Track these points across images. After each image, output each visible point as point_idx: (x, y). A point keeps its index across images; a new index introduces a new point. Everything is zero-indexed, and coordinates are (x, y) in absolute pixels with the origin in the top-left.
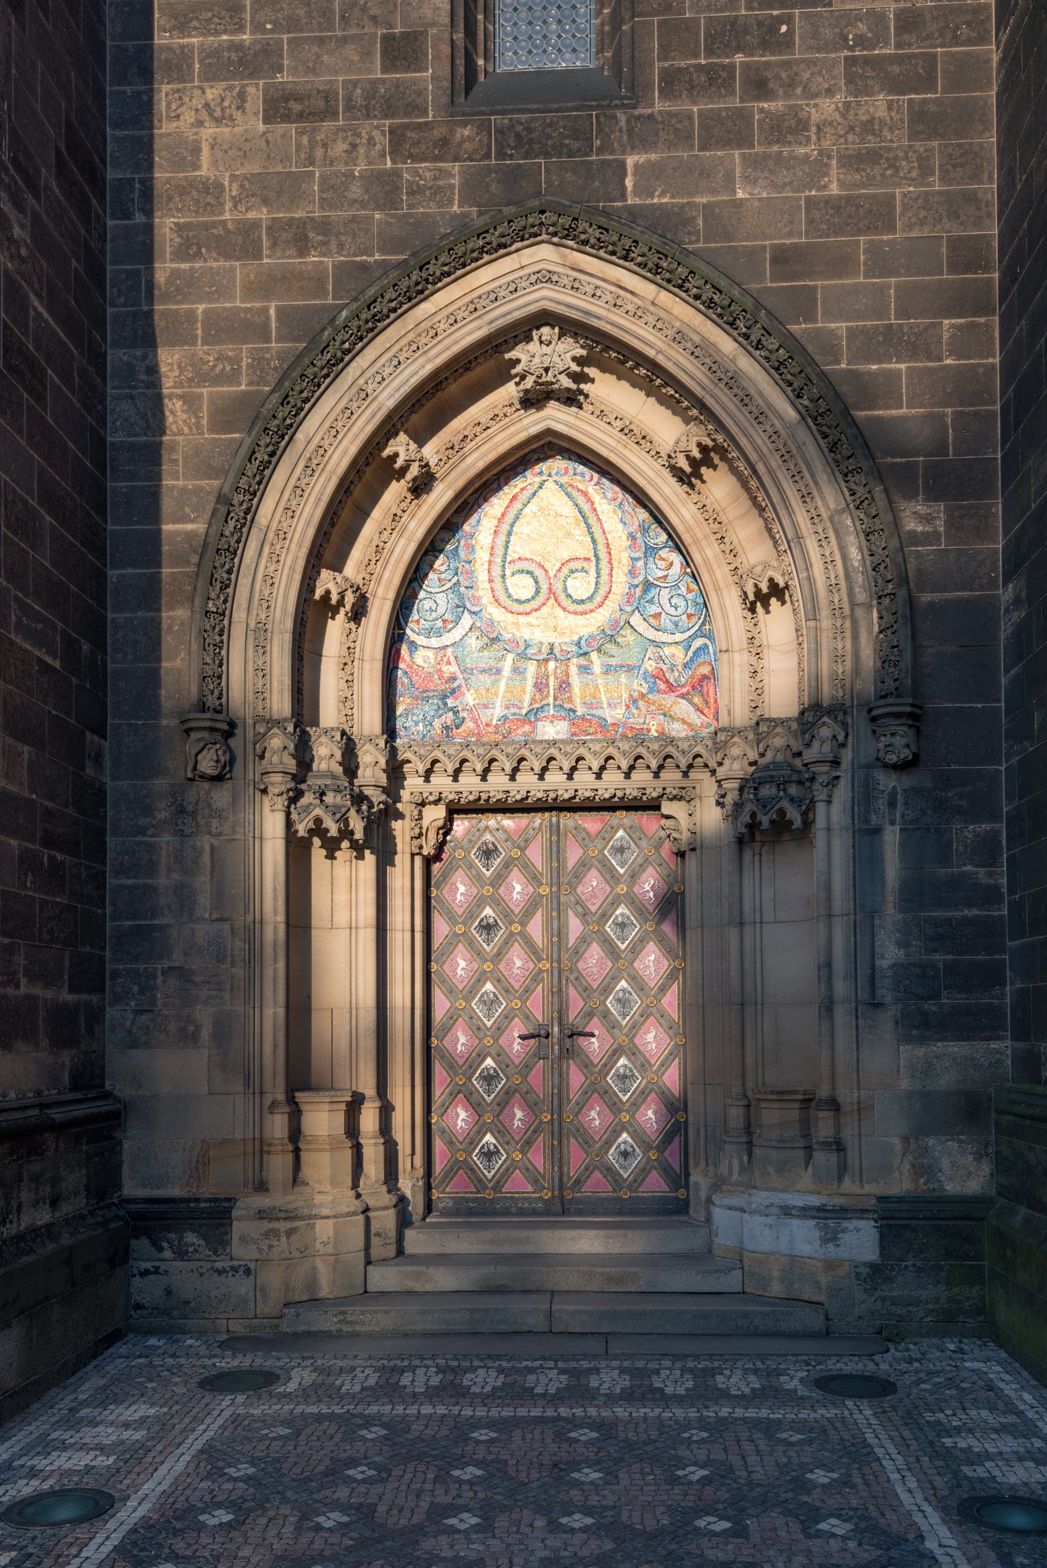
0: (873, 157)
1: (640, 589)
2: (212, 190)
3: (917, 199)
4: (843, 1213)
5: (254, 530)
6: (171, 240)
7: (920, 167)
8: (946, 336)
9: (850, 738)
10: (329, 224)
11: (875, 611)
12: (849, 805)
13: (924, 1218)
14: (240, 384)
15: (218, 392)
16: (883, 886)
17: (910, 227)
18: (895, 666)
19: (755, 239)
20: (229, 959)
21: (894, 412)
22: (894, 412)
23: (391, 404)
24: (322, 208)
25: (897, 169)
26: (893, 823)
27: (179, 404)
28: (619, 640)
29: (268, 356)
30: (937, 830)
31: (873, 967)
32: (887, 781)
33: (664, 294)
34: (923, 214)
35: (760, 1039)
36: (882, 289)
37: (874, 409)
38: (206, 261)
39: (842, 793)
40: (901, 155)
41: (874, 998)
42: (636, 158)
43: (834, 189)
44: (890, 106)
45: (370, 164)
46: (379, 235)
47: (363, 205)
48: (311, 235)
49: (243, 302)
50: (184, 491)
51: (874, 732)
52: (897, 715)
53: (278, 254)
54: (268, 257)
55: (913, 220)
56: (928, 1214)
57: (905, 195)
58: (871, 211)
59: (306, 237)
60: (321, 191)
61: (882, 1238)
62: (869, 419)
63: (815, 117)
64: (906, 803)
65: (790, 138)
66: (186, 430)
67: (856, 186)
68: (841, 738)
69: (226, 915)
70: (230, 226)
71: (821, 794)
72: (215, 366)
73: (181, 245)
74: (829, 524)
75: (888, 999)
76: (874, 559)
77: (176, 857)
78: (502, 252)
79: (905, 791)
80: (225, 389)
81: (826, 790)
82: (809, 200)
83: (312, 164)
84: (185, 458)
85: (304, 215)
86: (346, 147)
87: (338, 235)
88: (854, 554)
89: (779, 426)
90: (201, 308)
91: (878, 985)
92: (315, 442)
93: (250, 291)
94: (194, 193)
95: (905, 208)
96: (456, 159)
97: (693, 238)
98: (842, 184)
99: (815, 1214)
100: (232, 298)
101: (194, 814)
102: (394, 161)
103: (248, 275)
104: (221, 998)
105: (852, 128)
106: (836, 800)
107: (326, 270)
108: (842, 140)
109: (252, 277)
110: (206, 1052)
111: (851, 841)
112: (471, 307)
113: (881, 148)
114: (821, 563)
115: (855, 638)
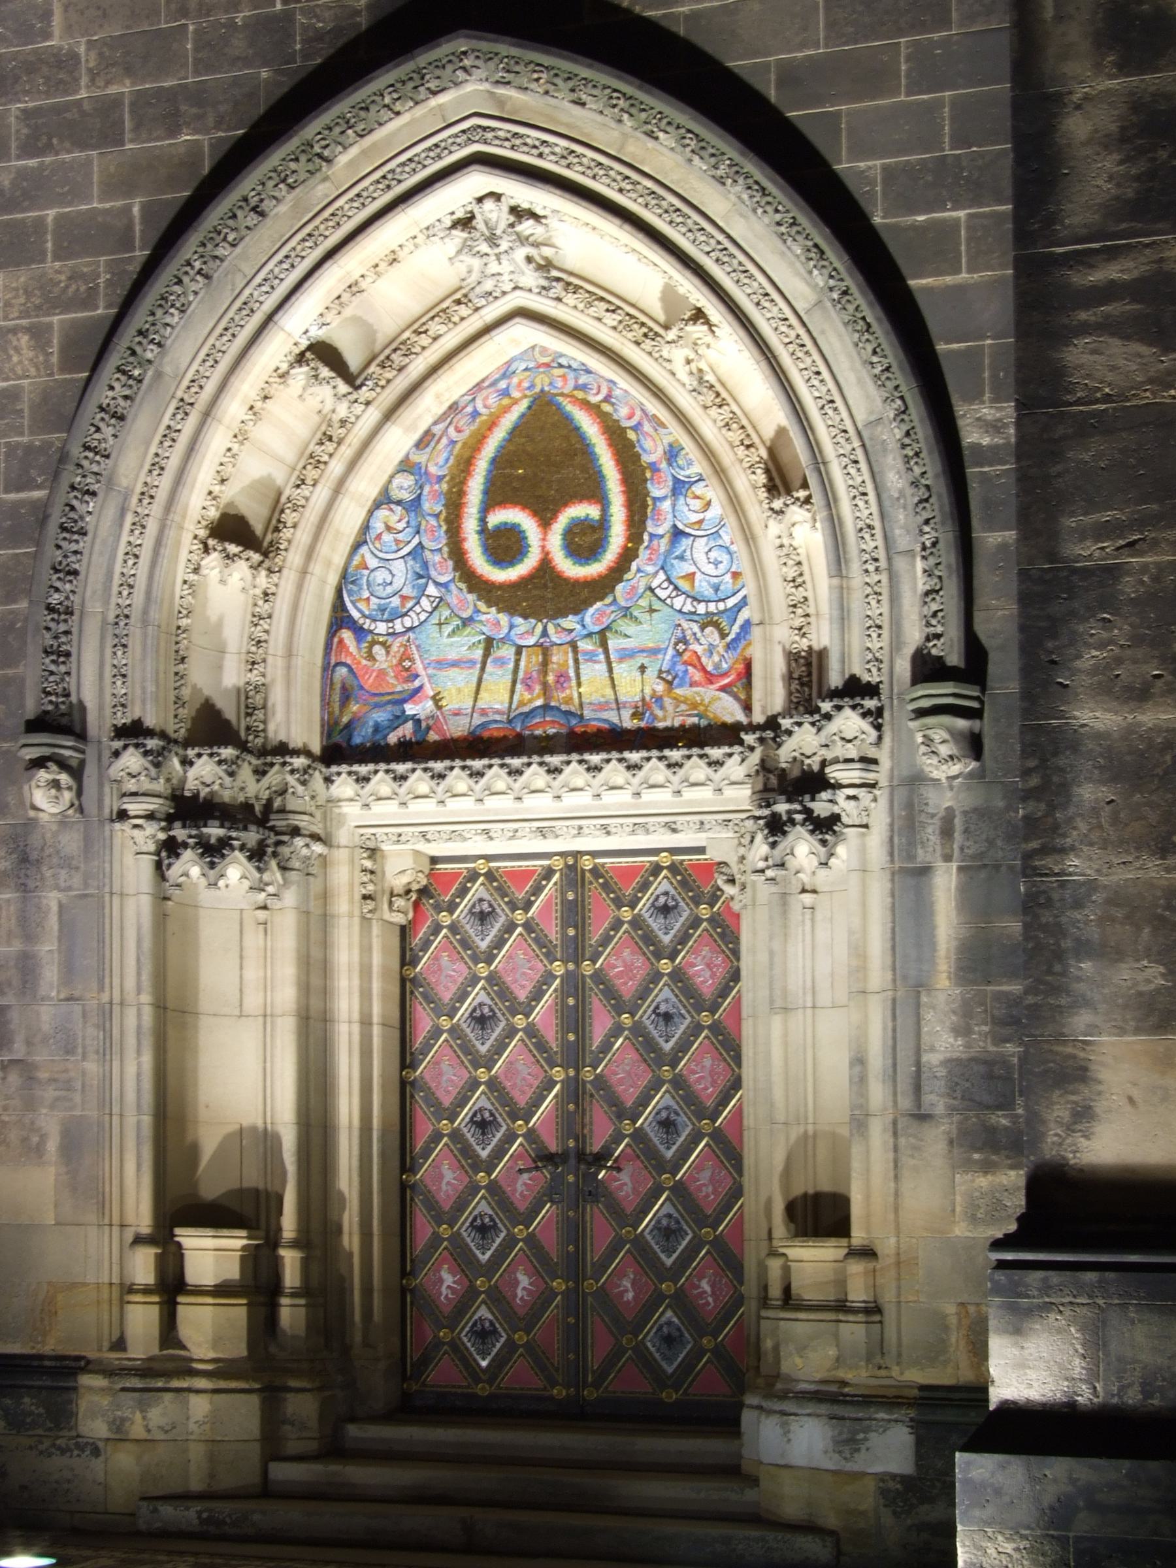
2: (66, 62)
6: (18, 131)
14: (97, 308)
21: (949, 280)
22: (949, 280)
26: (948, 858)
31: (918, 1064)
41: (919, 1107)
49: (101, 201)
54: (132, 141)
64: (966, 831)
70: (86, 106)
72: (67, 287)
73: (27, 136)
79: (965, 813)
88: (895, 480)
90: (51, 214)
91: (925, 1088)
94: (45, 70)
100: (88, 198)
111: (889, 885)
115: (895, 599)
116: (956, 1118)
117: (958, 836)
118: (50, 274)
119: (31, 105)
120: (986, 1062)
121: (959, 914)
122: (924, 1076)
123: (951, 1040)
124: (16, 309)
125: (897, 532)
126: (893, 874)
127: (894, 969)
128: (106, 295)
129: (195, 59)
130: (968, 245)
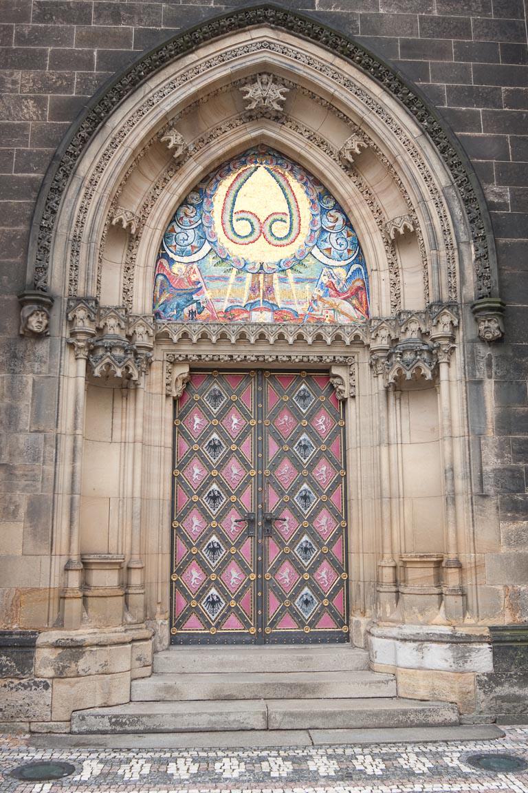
1: (318, 232)
3: (482, 23)
4: (468, 640)
5: (75, 179)
6: (34, 11)
8: (503, 96)
9: (461, 323)
10: (133, 8)
11: (472, 246)
12: (463, 365)
13: (522, 641)
14: (72, 93)
16: (486, 418)
17: (479, 36)
18: (487, 279)
19: (392, 35)
20: (42, 459)
21: (477, 134)
22: (477, 134)
23: (168, 108)
25: (470, 7)
26: (490, 377)
28: (306, 263)
29: (91, 78)
30: (517, 383)
31: (481, 471)
32: (484, 351)
34: (486, 30)
35: (402, 521)
36: (466, 68)
37: (465, 131)
38: (55, 23)
39: (458, 356)
41: (483, 492)
43: (435, 13)
48: (122, 13)
49: (76, 47)
50: (30, 153)
51: (476, 320)
52: (491, 309)
53: (101, 22)
54: (94, 23)
55: (481, 33)
56: (523, 638)
57: (475, 20)
58: (456, 26)
61: (494, 655)
62: (461, 136)
66: (35, 117)
67: (446, 13)
68: (455, 323)
69: (41, 428)
71: (443, 359)
72: (56, 82)
74: (441, 194)
75: (492, 492)
76: (473, 215)
77: (8, 387)
78: (240, 29)
79: (496, 357)
80: (62, 95)
81: (447, 356)
82: (421, 18)
84: (33, 135)
87: (139, 14)
89: (409, 136)
90: (50, 49)
91: (485, 483)
92: (119, 128)
93: (81, 41)
95: (475, 26)
97: (355, 31)
98: (439, 11)
99: (449, 639)
103: (81, 32)
104: (35, 486)
106: (452, 363)
107: (131, 32)
109: (84, 33)
110: (22, 524)
111: (464, 388)
112: (220, 59)
114: (438, 217)
116: (499, 496)
117: (494, 368)
120: (511, 471)
122: (484, 477)
123: (496, 460)
125: (461, 234)
126: (466, 382)
127: (468, 427)
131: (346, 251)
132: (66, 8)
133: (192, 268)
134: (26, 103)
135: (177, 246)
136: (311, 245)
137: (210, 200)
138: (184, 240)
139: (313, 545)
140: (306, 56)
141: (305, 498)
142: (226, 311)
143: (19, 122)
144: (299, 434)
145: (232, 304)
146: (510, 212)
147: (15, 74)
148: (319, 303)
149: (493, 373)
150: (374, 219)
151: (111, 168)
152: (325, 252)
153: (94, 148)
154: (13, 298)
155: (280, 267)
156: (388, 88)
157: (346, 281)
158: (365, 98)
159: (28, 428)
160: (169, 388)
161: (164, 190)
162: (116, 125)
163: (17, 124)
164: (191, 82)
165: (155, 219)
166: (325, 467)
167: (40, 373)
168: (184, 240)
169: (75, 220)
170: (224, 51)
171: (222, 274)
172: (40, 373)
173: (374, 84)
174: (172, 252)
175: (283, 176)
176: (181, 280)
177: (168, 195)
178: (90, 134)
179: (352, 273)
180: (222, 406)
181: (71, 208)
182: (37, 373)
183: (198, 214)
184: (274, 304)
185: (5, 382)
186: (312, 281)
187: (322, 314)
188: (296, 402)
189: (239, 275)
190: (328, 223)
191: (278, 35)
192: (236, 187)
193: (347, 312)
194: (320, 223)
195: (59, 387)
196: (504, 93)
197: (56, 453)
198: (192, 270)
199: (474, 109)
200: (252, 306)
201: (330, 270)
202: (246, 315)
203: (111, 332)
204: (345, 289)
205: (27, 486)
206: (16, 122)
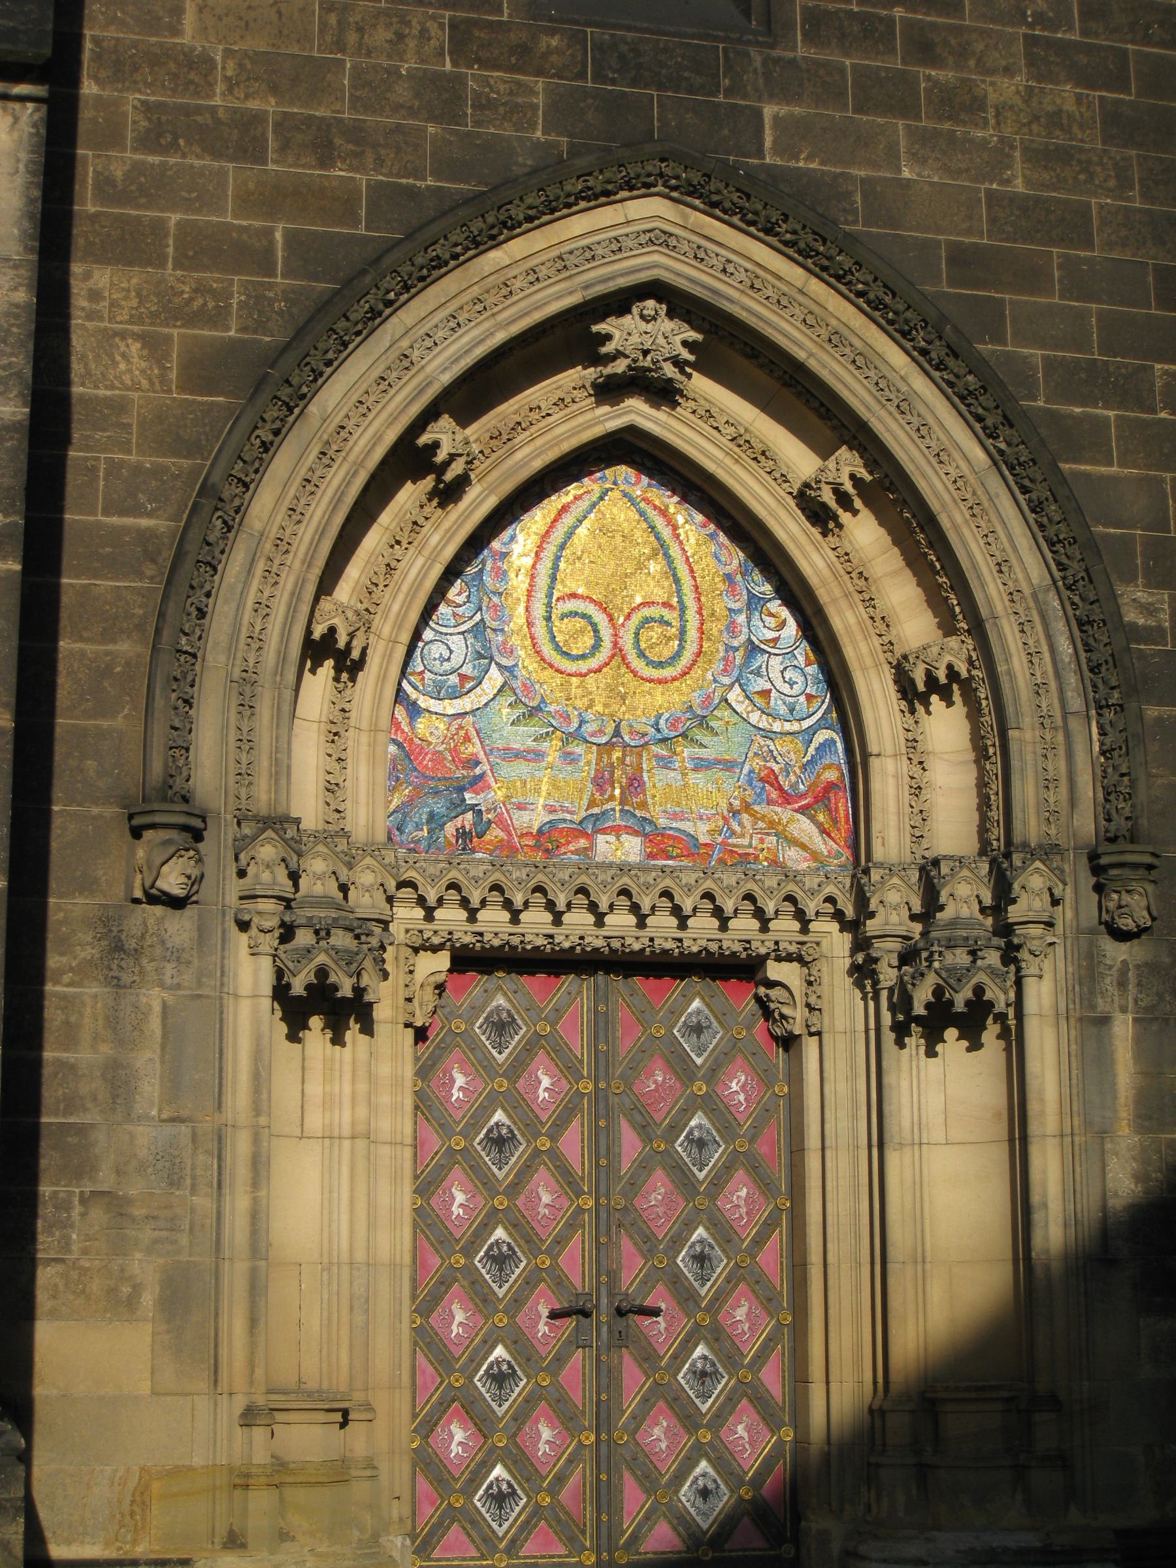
0: (1063, 156)
5: (242, 536)
6: (134, 122)
7: (1118, 177)
14: (228, 329)
15: (195, 337)
17: (1110, 245)
20: (188, 1182)
22: (1103, 469)
24: (353, 108)
25: (1091, 176)
26: (1124, 1010)
27: (135, 347)
29: (271, 295)
33: (814, 281)
37: (1080, 463)
38: (184, 156)
40: (1095, 159)
42: (776, 108)
43: (1019, 186)
44: (1079, 99)
45: (422, 62)
46: (433, 155)
47: (412, 113)
48: (338, 141)
49: (236, 217)
50: (137, 469)
53: (290, 160)
54: (275, 162)
55: (1113, 237)
57: (1101, 207)
59: (331, 143)
60: (353, 86)
63: (992, 97)
64: (1139, 984)
65: (963, 116)
66: (145, 383)
69: (184, 1113)
70: (221, 114)
72: (191, 300)
74: (1032, 604)
77: (107, 1018)
78: (603, 200)
82: (990, 194)
83: (342, 50)
85: (329, 114)
86: (390, 35)
88: (1065, 647)
90: (174, 218)
92: (337, 421)
93: (247, 203)
96: (539, 73)
97: (850, 218)
98: (1028, 182)
101: (137, 953)
102: (455, 63)
104: (175, 1242)
105: (1036, 118)
108: (1025, 130)
109: (251, 186)
110: (149, 1327)
113: (1072, 147)
117: (1132, 987)
118: (171, 281)
119: (152, 98)
121: (1135, 1064)
124: (126, 311)
125: (1069, 694)
128: (239, 317)
129: (351, 95)
130: (1117, 441)
131: (802, 699)
132: (209, 121)
133: (461, 727)
134: (123, 348)
135: (427, 675)
136: (727, 681)
137: (499, 564)
138: (444, 660)
139: (718, 1365)
140: (746, 271)
141: (701, 1259)
142: (540, 831)
143: (108, 393)
144: (687, 1112)
145: (552, 817)
146: (1169, 648)
147: (96, 274)
148: (745, 817)
149: (1131, 1005)
150: (876, 639)
151: (319, 512)
152: (757, 699)
153: (281, 464)
154: (110, 811)
155: (658, 730)
156: (921, 355)
157: (804, 767)
158: (872, 374)
159: (154, 1113)
160: (409, 1006)
161: (412, 549)
162: (330, 410)
163: (106, 398)
164: (493, 315)
165: (392, 616)
166: (745, 1190)
167: (179, 986)
168: (444, 660)
169: (244, 633)
170: (568, 248)
171: (530, 743)
172: (179, 986)
173: (891, 343)
174: (415, 688)
175: (664, 513)
176: (438, 757)
177: (420, 561)
178: (277, 433)
179: (817, 749)
180: (515, 1048)
181: (234, 605)
182: (170, 988)
183: (473, 599)
184: (645, 819)
185: (99, 1005)
186: (729, 766)
187: (750, 846)
188: (681, 1040)
189: (569, 749)
190: (765, 631)
191: (685, 217)
192: (558, 536)
193: (805, 840)
194: (745, 630)
195: (221, 1021)
196: (1161, 377)
197: (220, 1167)
198: (462, 733)
199: (1099, 411)
200: (596, 824)
201: (769, 742)
202: (583, 843)
203: (318, 889)
204: (801, 786)
205: (156, 1241)
206: (102, 392)
